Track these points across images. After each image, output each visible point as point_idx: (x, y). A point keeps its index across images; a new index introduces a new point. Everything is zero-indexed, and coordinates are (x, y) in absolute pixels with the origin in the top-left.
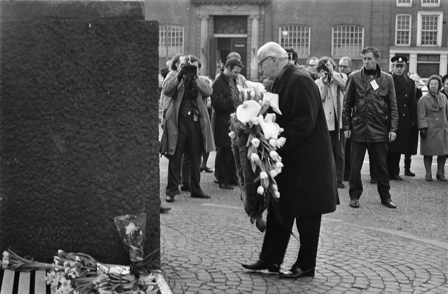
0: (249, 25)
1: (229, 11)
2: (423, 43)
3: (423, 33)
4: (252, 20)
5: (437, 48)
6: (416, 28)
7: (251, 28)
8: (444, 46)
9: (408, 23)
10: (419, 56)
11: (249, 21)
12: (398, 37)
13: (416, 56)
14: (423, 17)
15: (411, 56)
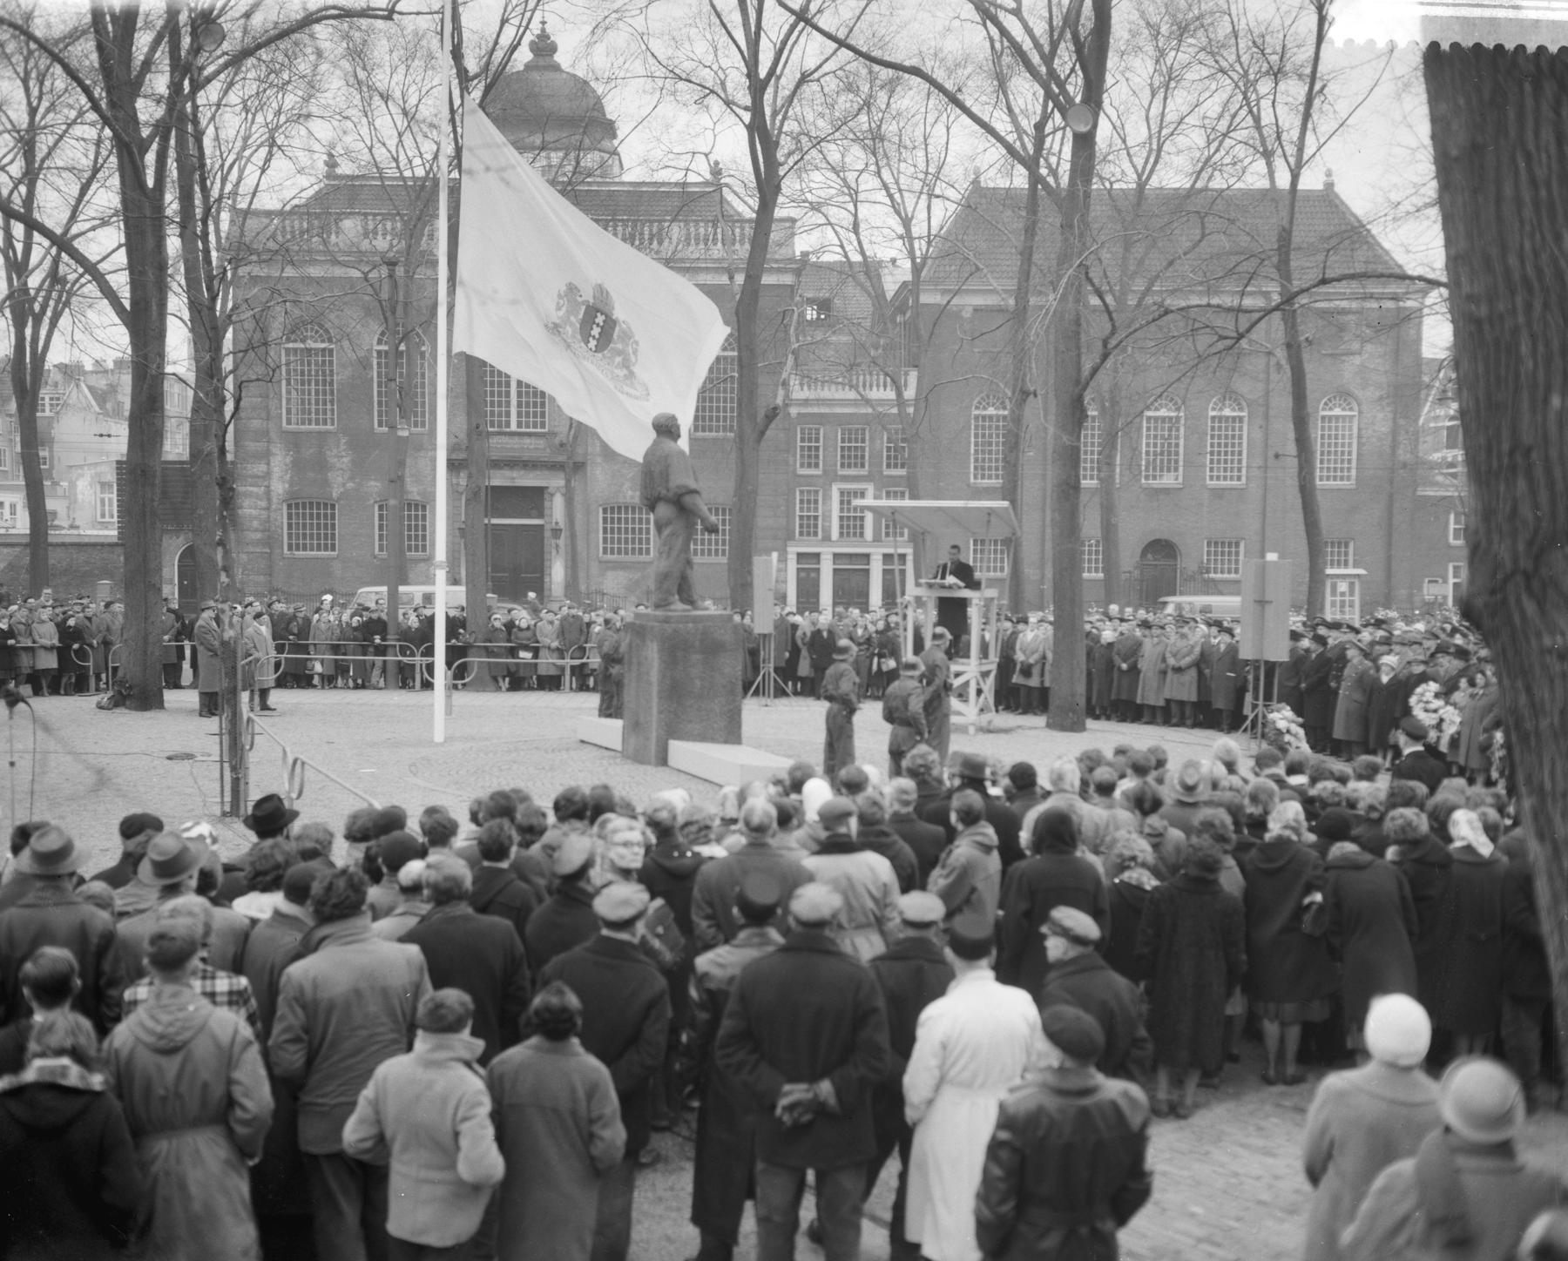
0: (547, 504)
2: (841, 534)
3: (841, 518)
4: (552, 495)
5: (865, 544)
8: (877, 539)
9: (816, 502)
10: (836, 556)
12: (801, 526)
14: (842, 493)
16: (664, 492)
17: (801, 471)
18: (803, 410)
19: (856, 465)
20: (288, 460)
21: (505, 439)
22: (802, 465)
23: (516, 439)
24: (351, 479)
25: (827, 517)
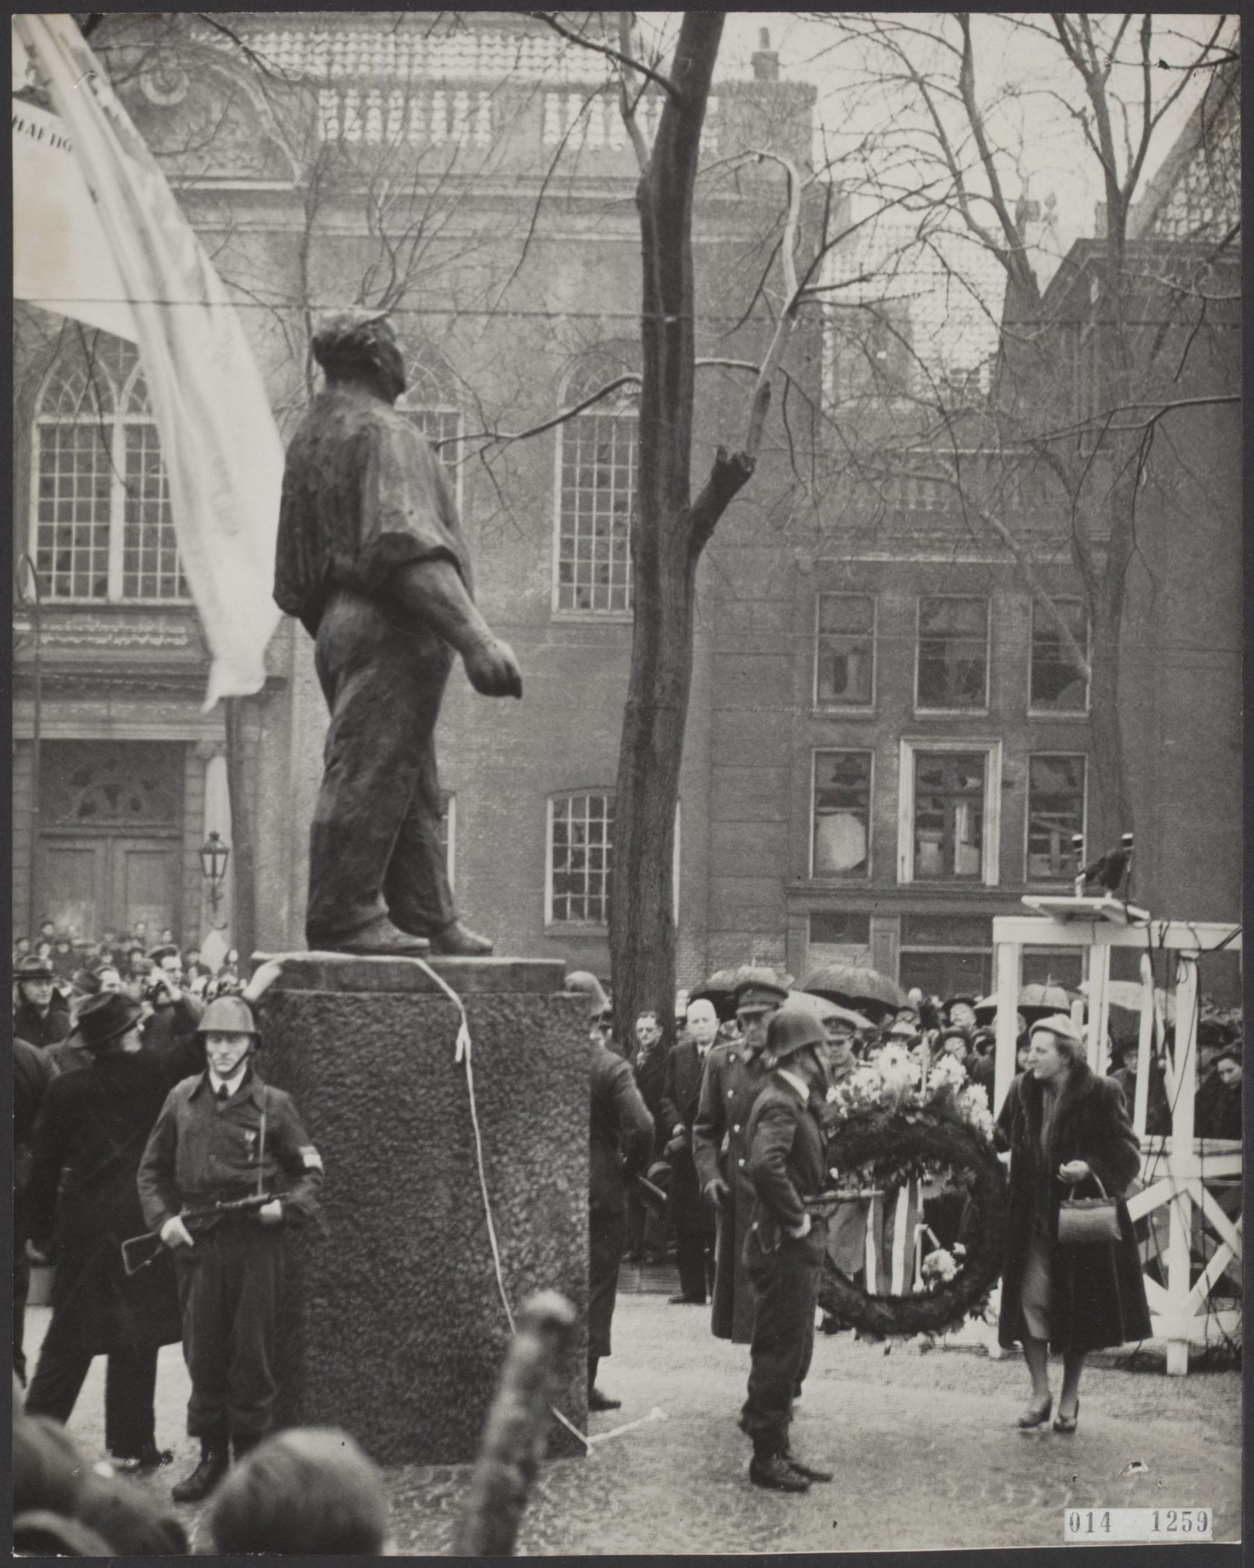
0: (192, 785)
1: (109, 721)
4: (204, 762)
7: (202, 795)
11: (191, 769)
16: (344, 561)
21: (94, 624)
23: (121, 624)
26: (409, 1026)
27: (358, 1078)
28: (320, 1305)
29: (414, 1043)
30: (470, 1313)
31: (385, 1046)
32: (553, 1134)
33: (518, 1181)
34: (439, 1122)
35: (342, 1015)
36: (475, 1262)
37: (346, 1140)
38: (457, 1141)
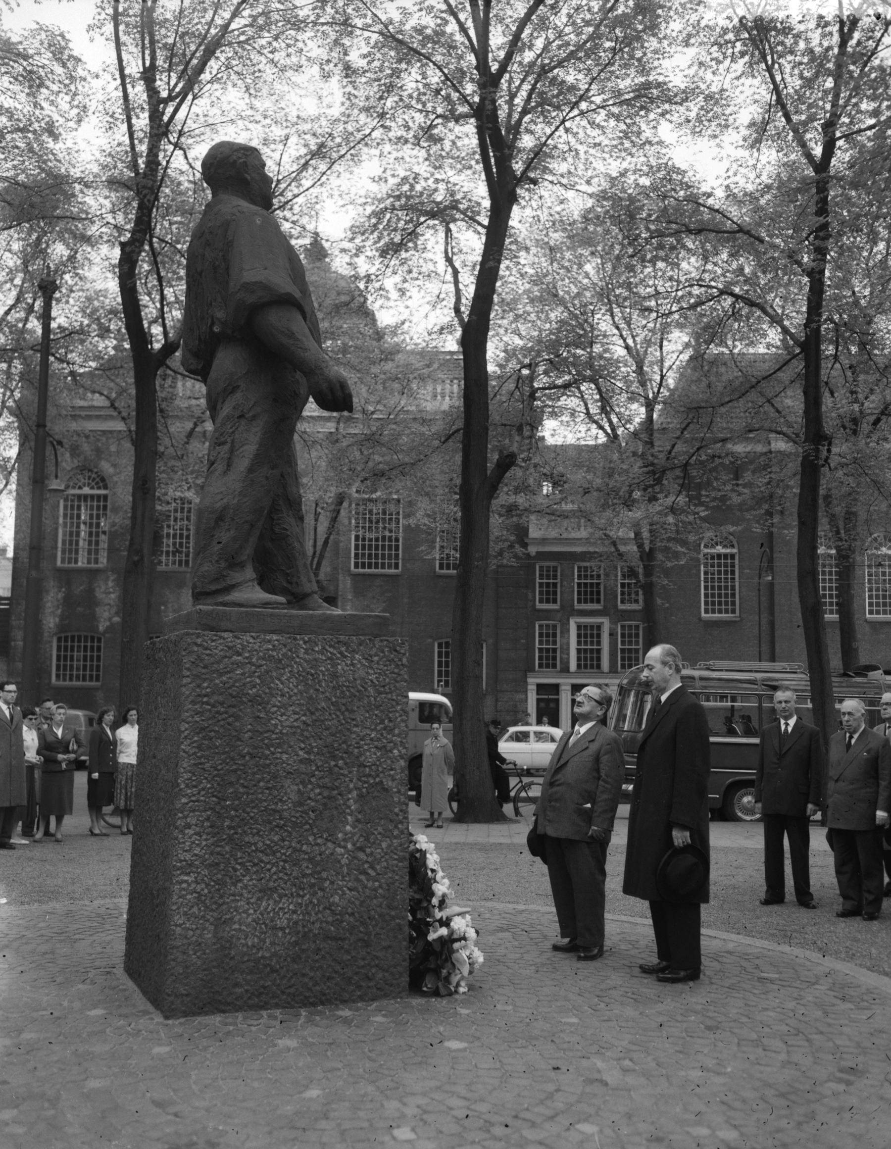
2: (579, 666)
6: (568, 644)
8: (613, 670)
9: (555, 635)
12: (540, 658)
13: (569, 688)
14: (579, 627)
15: (562, 688)
17: (539, 606)
18: (541, 549)
19: (592, 601)
20: (60, 596)
22: (541, 601)
24: (117, 614)
25: (566, 649)
26: (263, 659)
27: (221, 698)
28: (186, 881)
29: (267, 672)
30: (312, 886)
31: (243, 674)
32: (379, 744)
33: (351, 781)
34: (287, 734)
35: (206, 649)
36: (318, 844)
37: (209, 748)
38: (302, 749)
